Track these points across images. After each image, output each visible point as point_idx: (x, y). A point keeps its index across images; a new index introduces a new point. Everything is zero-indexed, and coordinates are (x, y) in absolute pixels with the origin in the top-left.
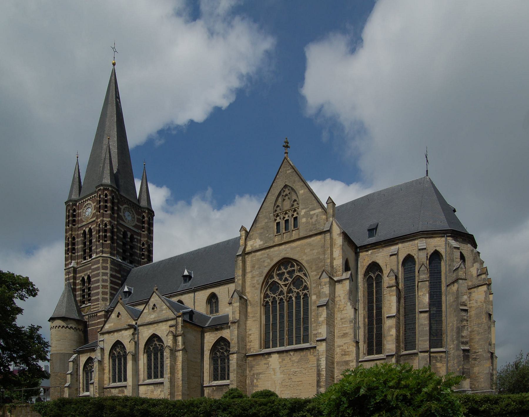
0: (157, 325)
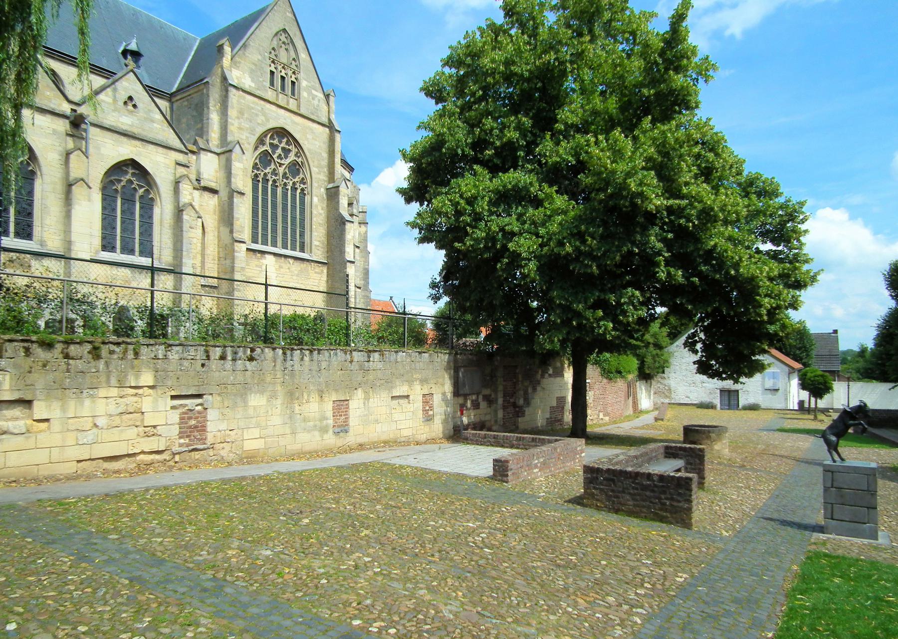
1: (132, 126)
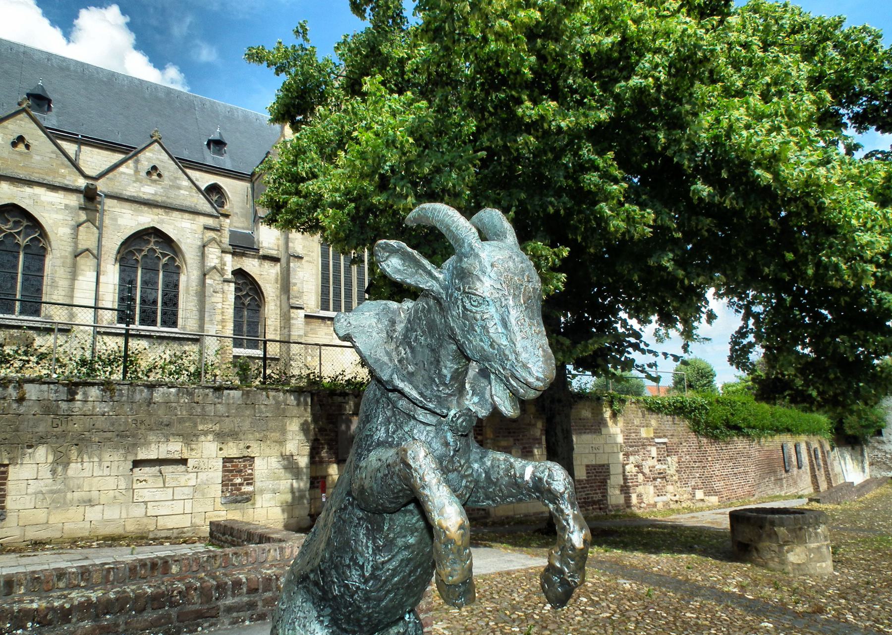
0: (167, 214)
1: (155, 194)
